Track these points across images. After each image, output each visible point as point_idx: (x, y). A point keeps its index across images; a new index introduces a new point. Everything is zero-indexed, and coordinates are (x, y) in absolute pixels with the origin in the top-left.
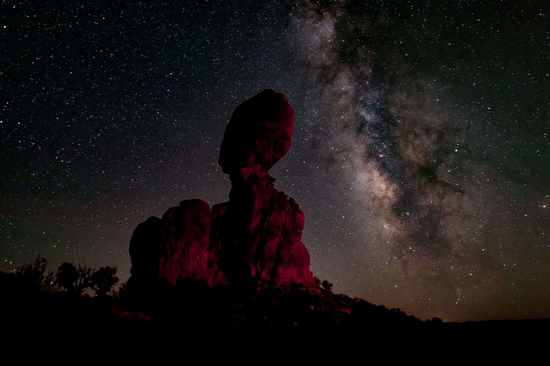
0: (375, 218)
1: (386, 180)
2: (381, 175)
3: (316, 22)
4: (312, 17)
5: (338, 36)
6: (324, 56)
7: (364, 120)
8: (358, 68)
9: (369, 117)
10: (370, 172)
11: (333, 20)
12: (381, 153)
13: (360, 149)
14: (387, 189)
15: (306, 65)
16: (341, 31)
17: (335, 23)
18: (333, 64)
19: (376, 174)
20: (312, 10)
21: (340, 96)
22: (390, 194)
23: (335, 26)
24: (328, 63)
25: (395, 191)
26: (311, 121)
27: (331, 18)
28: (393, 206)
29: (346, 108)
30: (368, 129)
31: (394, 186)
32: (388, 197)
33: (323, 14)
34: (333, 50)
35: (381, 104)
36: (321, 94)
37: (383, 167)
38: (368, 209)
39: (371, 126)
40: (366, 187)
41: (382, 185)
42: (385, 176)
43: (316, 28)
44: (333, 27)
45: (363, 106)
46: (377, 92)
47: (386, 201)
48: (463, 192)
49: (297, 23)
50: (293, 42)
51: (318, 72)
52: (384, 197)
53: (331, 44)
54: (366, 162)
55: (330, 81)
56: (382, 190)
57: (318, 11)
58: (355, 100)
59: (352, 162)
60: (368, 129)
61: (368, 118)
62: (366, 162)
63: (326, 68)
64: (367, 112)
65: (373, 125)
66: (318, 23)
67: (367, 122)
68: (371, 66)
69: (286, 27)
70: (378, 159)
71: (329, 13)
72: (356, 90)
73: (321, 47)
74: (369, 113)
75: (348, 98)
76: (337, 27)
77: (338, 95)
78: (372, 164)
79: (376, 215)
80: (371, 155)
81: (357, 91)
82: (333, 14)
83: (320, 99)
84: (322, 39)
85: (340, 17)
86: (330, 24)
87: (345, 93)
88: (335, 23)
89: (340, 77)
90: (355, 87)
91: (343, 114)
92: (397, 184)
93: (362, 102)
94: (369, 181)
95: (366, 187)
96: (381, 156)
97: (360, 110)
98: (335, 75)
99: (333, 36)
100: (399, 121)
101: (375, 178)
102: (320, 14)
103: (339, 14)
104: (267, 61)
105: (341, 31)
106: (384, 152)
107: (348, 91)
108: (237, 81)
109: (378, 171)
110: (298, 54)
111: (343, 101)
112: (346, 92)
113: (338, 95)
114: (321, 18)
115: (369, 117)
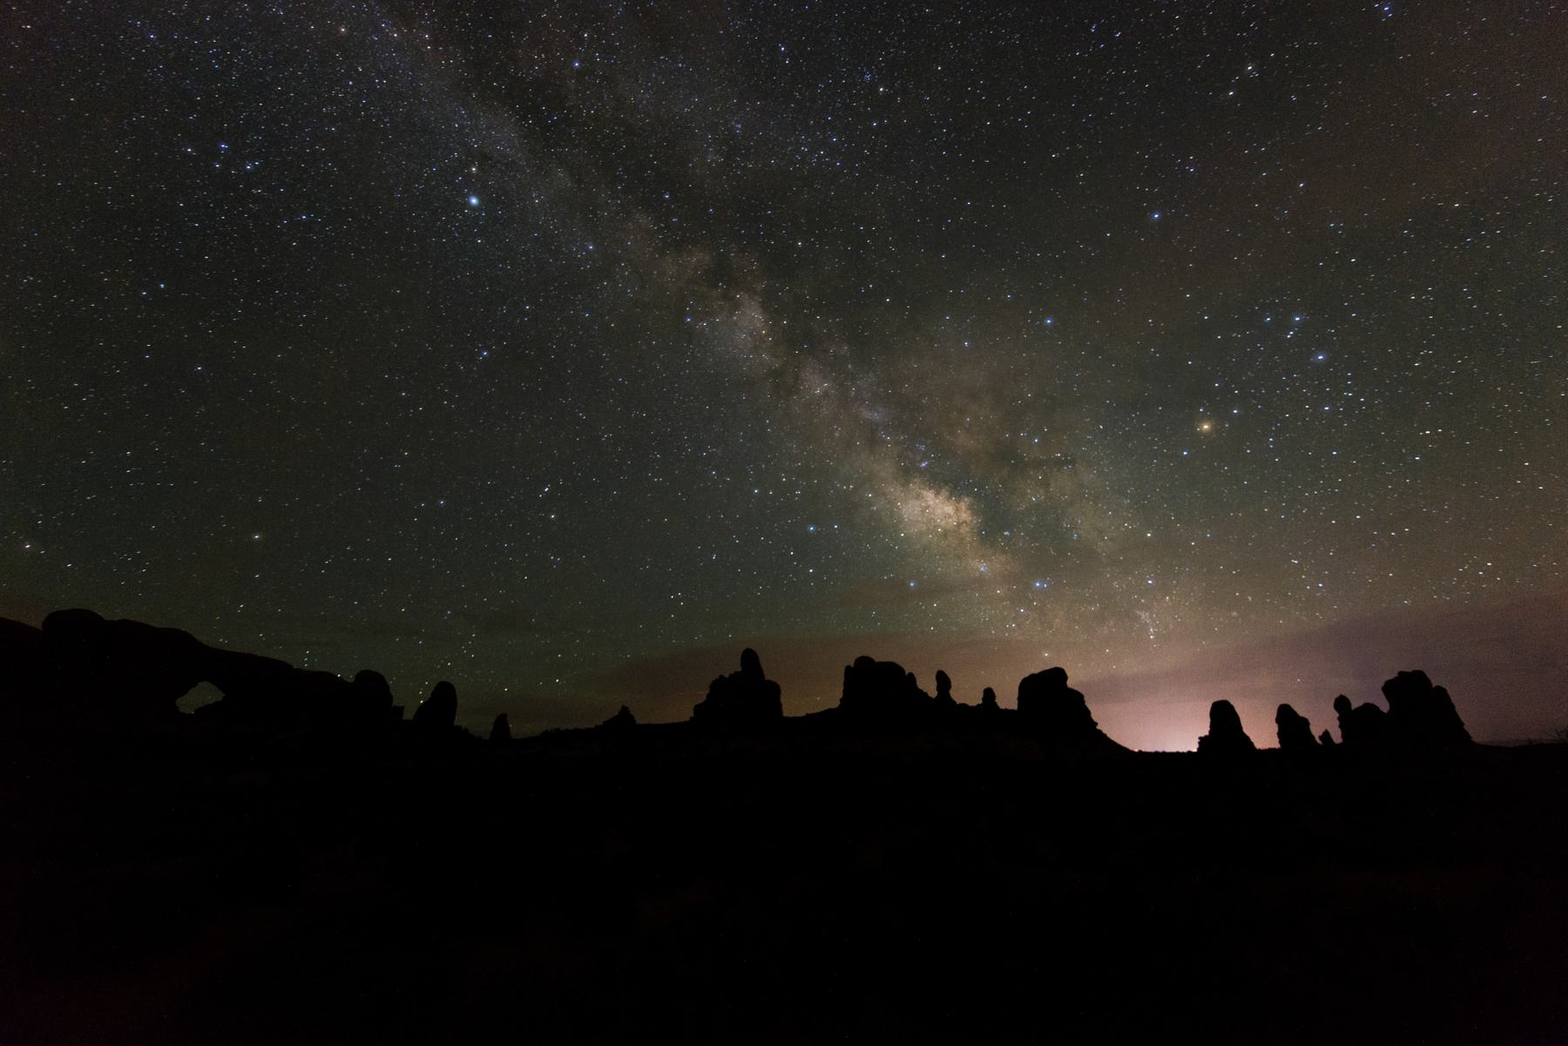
0: (961, 562)
1: (949, 498)
2: (937, 493)
3: (731, 314)
8: (826, 351)
9: (876, 416)
10: (918, 497)
11: (753, 300)
12: (922, 461)
13: (885, 469)
14: (957, 510)
17: (760, 302)
19: (929, 496)
21: (818, 405)
22: (965, 516)
25: (970, 507)
28: (979, 533)
31: (966, 502)
32: (965, 522)
37: (937, 480)
38: (943, 554)
40: (924, 523)
41: (946, 508)
42: (944, 493)
46: (871, 375)
47: (964, 529)
48: (1073, 462)
49: (704, 328)
52: (959, 525)
53: (767, 335)
54: (905, 484)
56: (950, 517)
57: (726, 296)
59: (884, 494)
61: (876, 416)
62: (905, 484)
69: (690, 343)
70: (922, 472)
76: (765, 307)
78: (914, 483)
79: (960, 558)
80: (906, 473)
88: (760, 302)
89: (806, 376)
92: (968, 496)
94: (923, 511)
95: (924, 523)
96: (924, 465)
101: (931, 503)
106: (925, 457)
108: (653, 454)
109: (930, 489)
110: (727, 371)
112: (826, 394)
114: (737, 305)
115: (876, 416)
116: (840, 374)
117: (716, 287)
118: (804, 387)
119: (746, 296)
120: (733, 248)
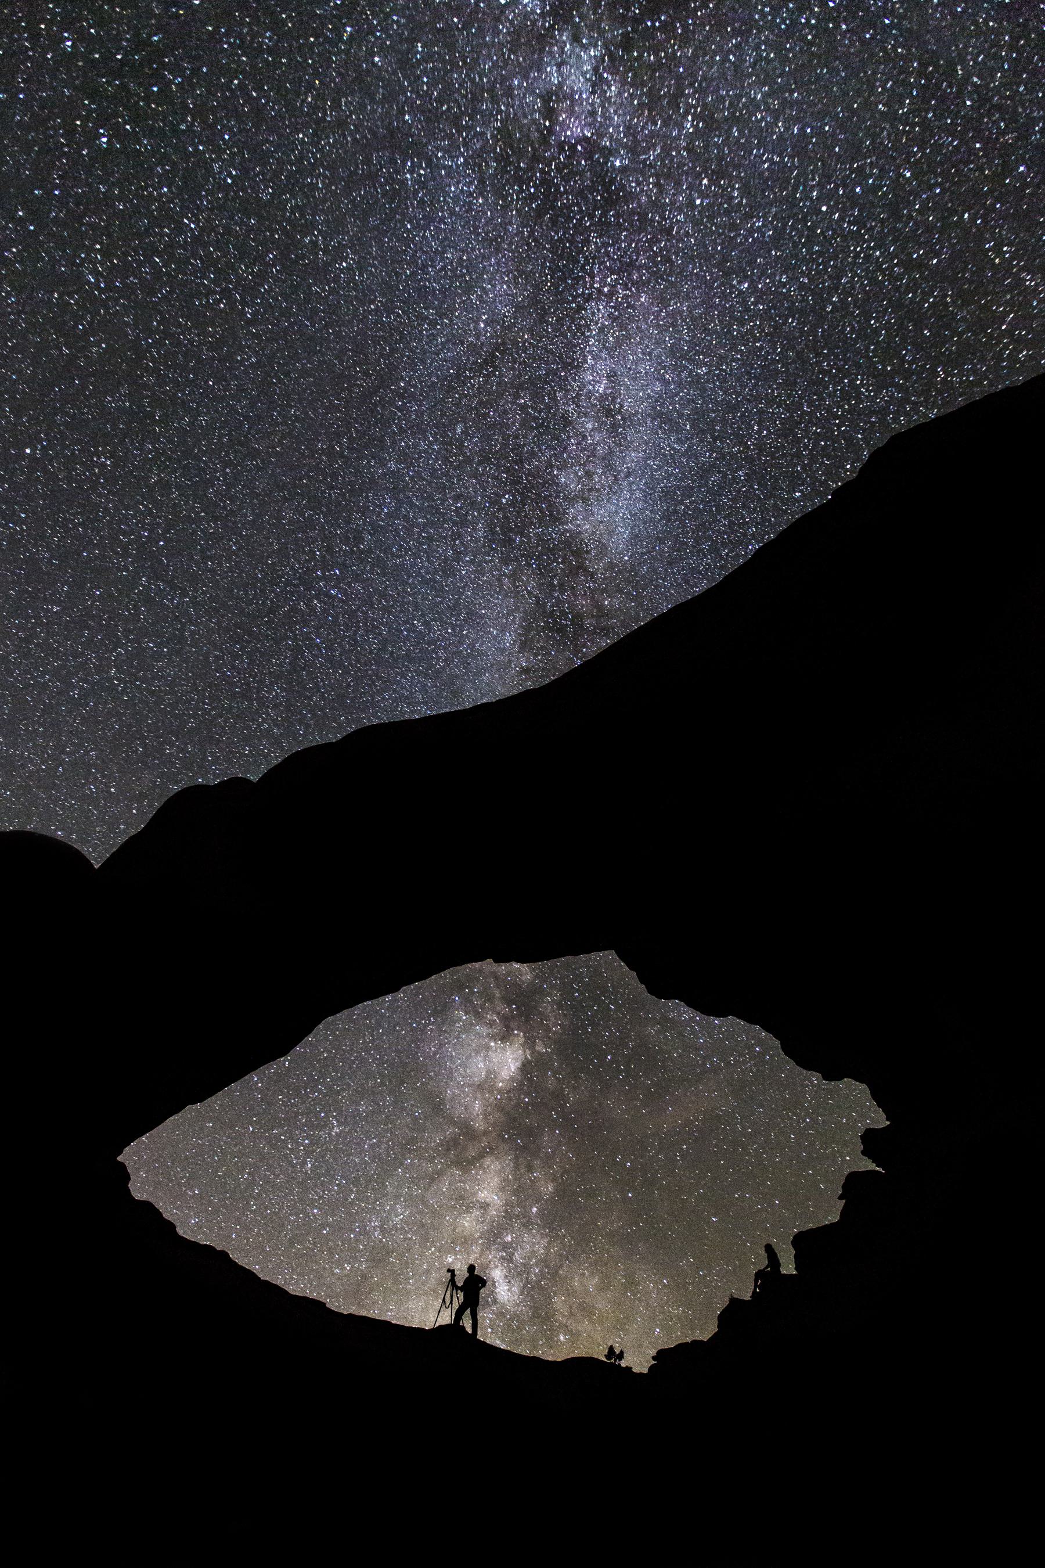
3: (493, 1037)
4: (491, 1024)
5: (521, 1084)
6: (477, 1106)
7: (493, 1292)
8: (530, 1168)
11: (525, 1051)
15: (436, 1106)
16: (530, 1080)
17: (526, 1058)
18: (486, 1133)
20: (498, 1014)
23: (524, 1065)
24: (479, 1125)
26: (383, 1230)
27: (523, 1047)
29: (466, 1242)
30: (490, 1320)
33: (513, 1030)
34: (499, 1107)
35: (542, 1275)
36: (432, 1180)
39: (501, 1314)
43: (488, 1048)
44: (518, 1064)
45: (502, 1257)
46: (544, 1242)
49: (460, 1019)
50: (434, 1046)
51: (451, 1131)
53: (500, 1091)
55: (466, 1164)
57: (506, 1020)
58: (493, 1237)
60: (490, 1320)
63: (468, 1131)
64: (506, 1277)
65: (503, 1314)
66: (495, 1041)
67: (495, 1301)
68: (554, 1180)
71: (525, 1037)
72: (506, 1212)
73: (480, 1087)
74: (509, 1282)
75: (482, 1222)
76: (525, 1068)
77: (464, 1202)
81: (508, 1215)
82: (530, 1043)
83: (427, 1190)
84: (488, 1072)
85: (539, 1053)
86: (515, 1056)
87: (481, 1207)
88: (526, 1058)
90: (506, 1205)
91: (456, 1254)
93: (505, 1247)
97: (495, 1262)
98: (481, 1156)
99: (512, 1078)
100: (562, 1338)
102: (509, 1029)
103: (540, 1048)
104: (367, 1052)
105: (530, 1080)
107: (488, 1205)
111: (468, 1223)
112: (485, 1206)
113: (464, 1202)
114: (505, 1037)
116: (518, 1206)
117: (509, 1005)
118: (477, 1174)
119: (522, 1040)
120: (556, 996)
